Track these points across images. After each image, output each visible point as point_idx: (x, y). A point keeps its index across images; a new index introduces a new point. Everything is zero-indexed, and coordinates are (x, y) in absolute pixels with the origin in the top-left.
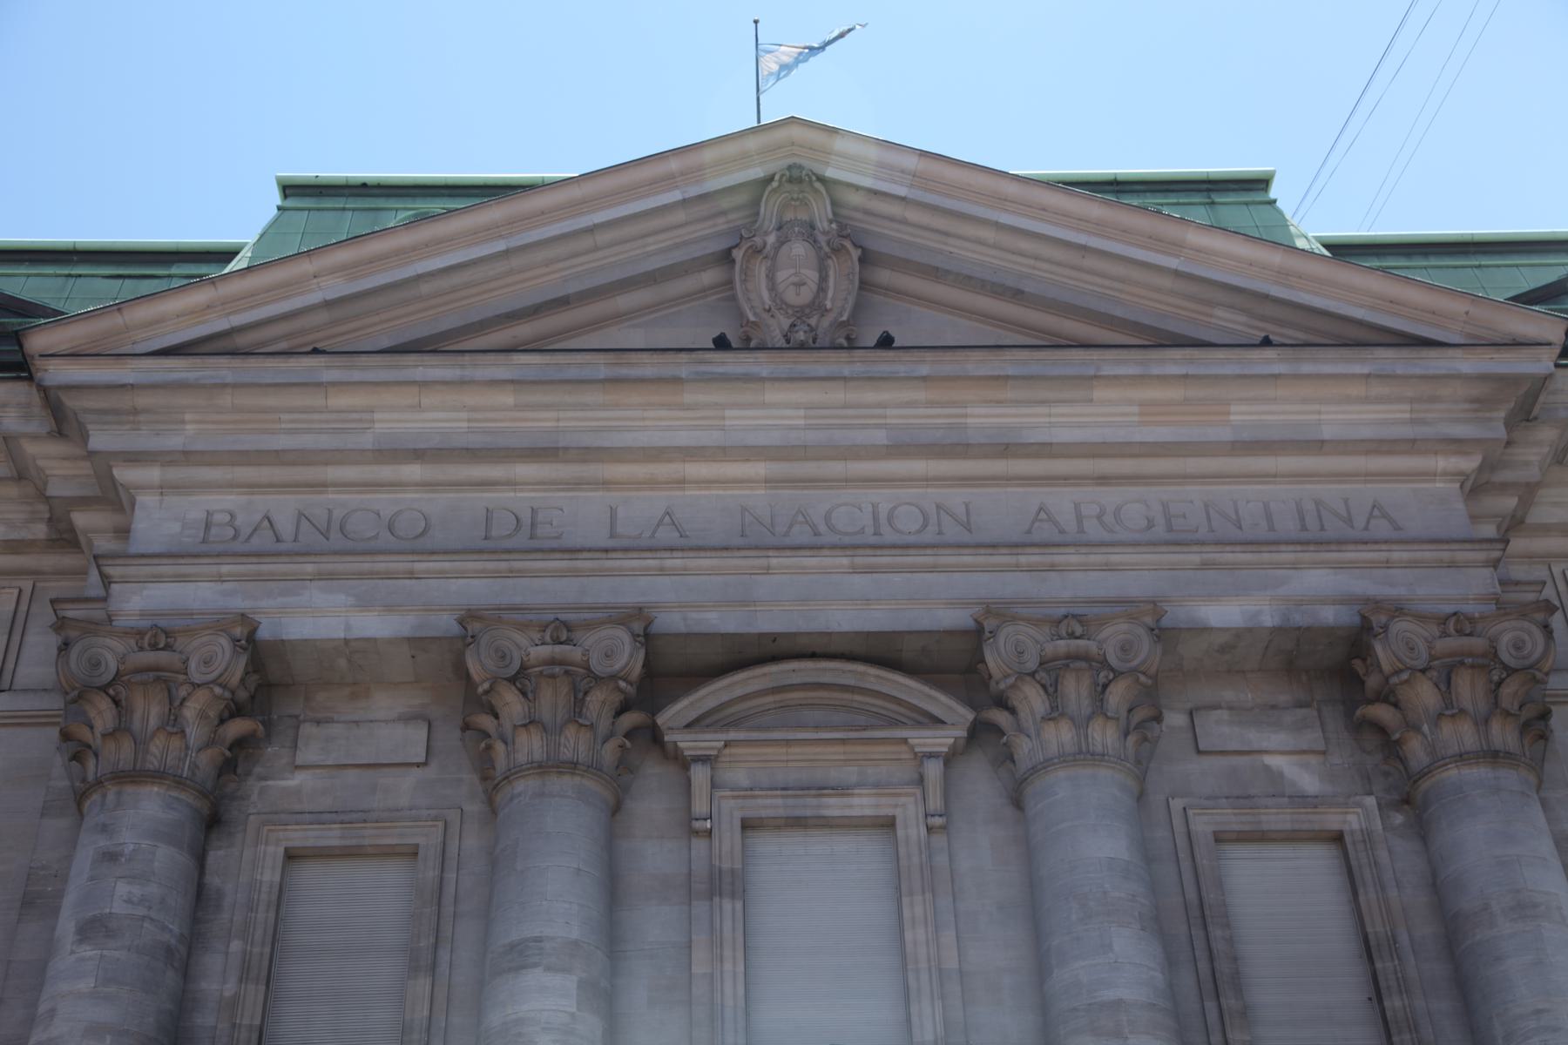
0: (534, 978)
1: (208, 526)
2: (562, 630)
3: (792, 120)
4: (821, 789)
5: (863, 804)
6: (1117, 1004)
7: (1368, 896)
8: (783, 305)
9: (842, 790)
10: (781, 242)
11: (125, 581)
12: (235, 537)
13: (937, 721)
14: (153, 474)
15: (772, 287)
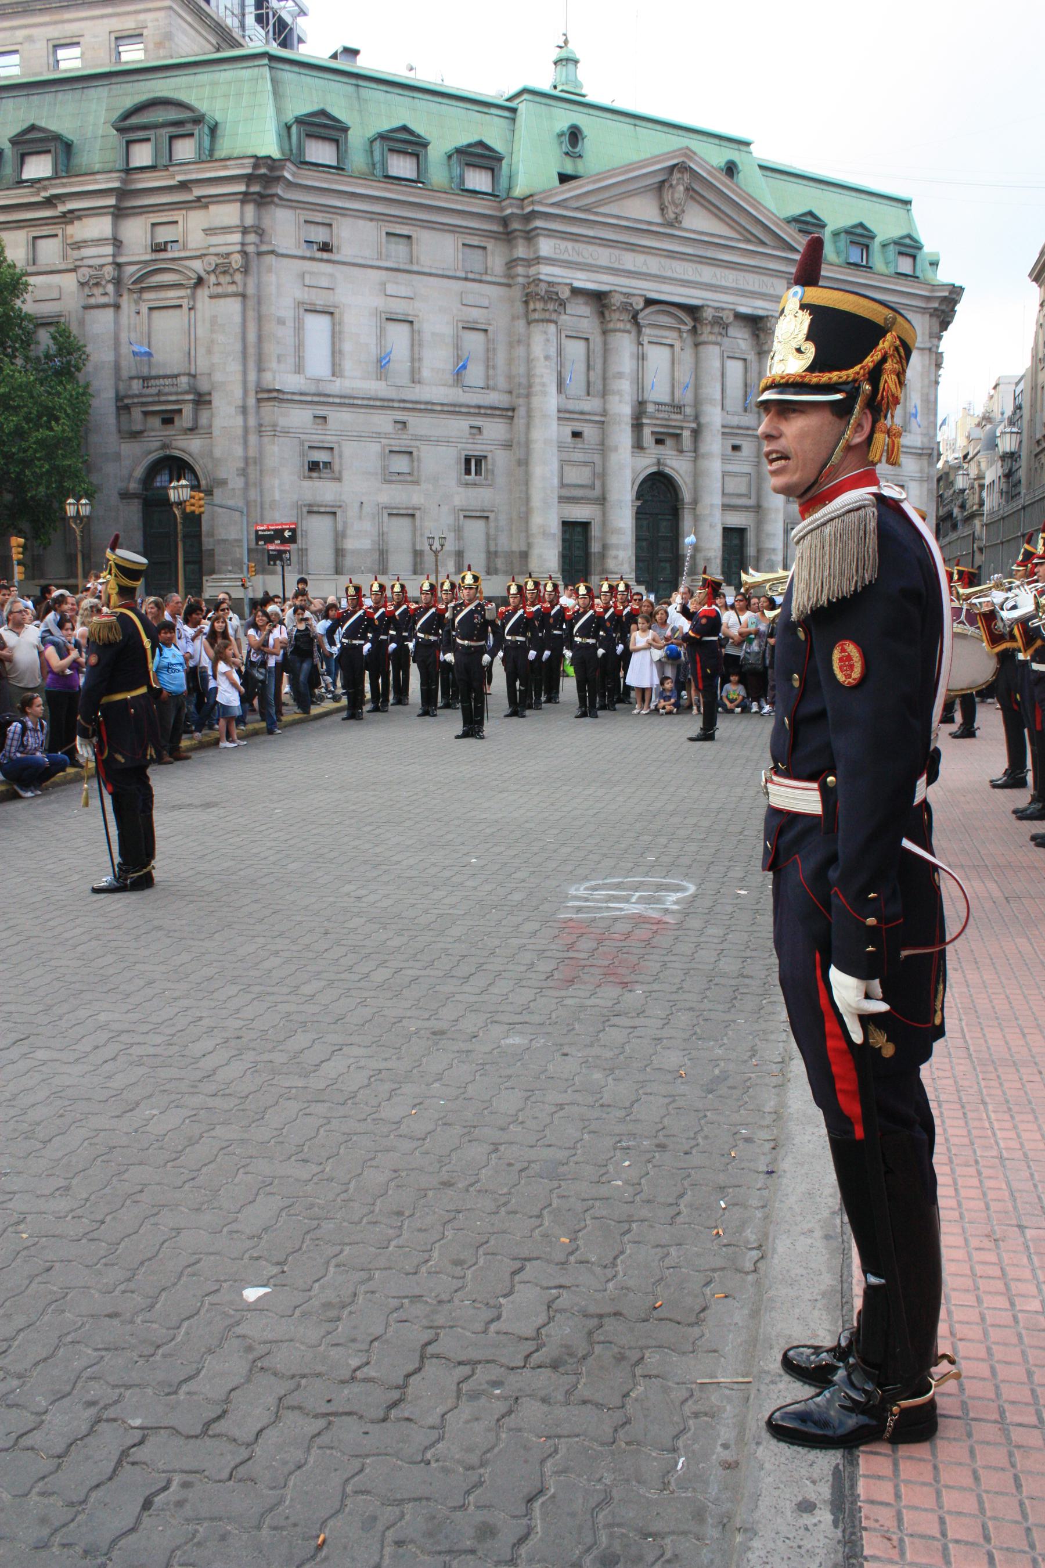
0: (623, 381)
2: (628, 295)
5: (669, 341)
7: (749, 374)
9: (667, 338)
10: (678, 184)
13: (686, 324)
14: (546, 232)
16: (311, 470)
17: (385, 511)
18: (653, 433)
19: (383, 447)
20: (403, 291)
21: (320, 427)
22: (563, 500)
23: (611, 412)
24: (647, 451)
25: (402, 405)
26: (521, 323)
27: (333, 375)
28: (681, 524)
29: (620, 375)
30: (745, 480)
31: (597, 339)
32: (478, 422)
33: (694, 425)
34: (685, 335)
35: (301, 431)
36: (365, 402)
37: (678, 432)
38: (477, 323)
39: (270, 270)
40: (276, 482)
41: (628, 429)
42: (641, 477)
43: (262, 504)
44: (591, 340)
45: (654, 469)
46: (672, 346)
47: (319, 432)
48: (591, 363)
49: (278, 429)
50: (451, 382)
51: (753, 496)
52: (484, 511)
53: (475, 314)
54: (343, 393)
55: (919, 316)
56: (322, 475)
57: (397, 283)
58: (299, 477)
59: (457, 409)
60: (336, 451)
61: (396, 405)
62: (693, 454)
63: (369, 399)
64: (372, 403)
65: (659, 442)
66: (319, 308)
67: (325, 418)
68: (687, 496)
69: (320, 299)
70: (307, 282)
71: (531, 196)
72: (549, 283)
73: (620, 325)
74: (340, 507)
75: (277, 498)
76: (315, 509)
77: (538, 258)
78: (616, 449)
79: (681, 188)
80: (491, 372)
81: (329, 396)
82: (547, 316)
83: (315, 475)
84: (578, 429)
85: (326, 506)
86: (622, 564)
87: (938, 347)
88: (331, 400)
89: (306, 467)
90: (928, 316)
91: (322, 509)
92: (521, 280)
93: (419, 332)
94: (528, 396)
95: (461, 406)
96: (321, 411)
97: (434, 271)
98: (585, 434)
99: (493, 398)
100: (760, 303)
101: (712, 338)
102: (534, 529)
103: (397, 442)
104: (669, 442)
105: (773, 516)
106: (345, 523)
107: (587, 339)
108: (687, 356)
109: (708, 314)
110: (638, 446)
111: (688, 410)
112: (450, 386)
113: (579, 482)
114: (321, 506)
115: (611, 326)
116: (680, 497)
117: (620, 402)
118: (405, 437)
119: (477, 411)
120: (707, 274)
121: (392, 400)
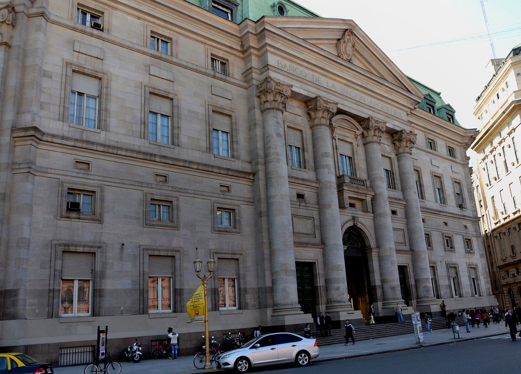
1: (278, 63)
3: (352, 21)
4: (346, 137)
6: (383, 177)
8: (347, 54)
11: (271, 70)
12: (282, 67)
15: (345, 49)
16: (69, 210)
17: (146, 252)
18: (350, 198)
19: (146, 195)
20: (165, 74)
21: (82, 171)
22: (298, 244)
23: (322, 180)
24: (346, 211)
25: (163, 160)
26: (257, 112)
27: (99, 128)
28: (369, 264)
29: (326, 155)
30: (401, 232)
31: (308, 132)
32: (228, 181)
33: (373, 194)
34: (359, 137)
35: (61, 172)
36: (129, 154)
37: (364, 198)
38: (224, 109)
39: (39, 28)
40: (26, 220)
41: (335, 191)
42: (345, 229)
43: (8, 242)
44: (304, 132)
45: (350, 224)
46: (351, 143)
47: (80, 175)
48: (305, 147)
49: (33, 167)
50: (204, 149)
51: (408, 244)
52: (235, 254)
53: (221, 102)
54: (108, 143)
55: (458, 147)
56: (81, 217)
57: (160, 68)
58: (56, 217)
59: (210, 169)
60: (98, 195)
61: (157, 159)
62: (372, 215)
63: (133, 151)
64: (135, 155)
65: (352, 205)
66: (89, 72)
67: (89, 164)
68: (372, 243)
69: (90, 65)
70: (77, 48)
71: (263, 17)
72: (277, 83)
73: (323, 121)
74: (100, 247)
75: (26, 233)
76: (72, 249)
77: (268, 64)
78: (329, 206)
79: (350, 45)
80: (235, 146)
81: (93, 143)
82: (275, 105)
83: (73, 215)
84: (301, 192)
85: (84, 246)
86: (343, 294)
87: (468, 164)
88: (95, 147)
89: (65, 208)
90: (462, 148)
91: (80, 249)
92: (255, 82)
93: (178, 107)
94: (266, 163)
95: (213, 167)
96: (84, 156)
97: (190, 65)
98: (306, 196)
99: (238, 165)
100: (396, 123)
101: (375, 139)
102: (278, 268)
103: (159, 191)
104: (358, 204)
105: (423, 256)
106: (104, 264)
107: (301, 131)
108: (360, 151)
109: (372, 123)
110: (342, 206)
111: (368, 183)
112: (203, 152)
113: (305, 231)
114: (79, 246)
115: (317, 121)
116: (367, 244)
117: (329, 173)
118: (165, 188)
119: (226, 172)
120: (368, 100)
121: (155, 155)
